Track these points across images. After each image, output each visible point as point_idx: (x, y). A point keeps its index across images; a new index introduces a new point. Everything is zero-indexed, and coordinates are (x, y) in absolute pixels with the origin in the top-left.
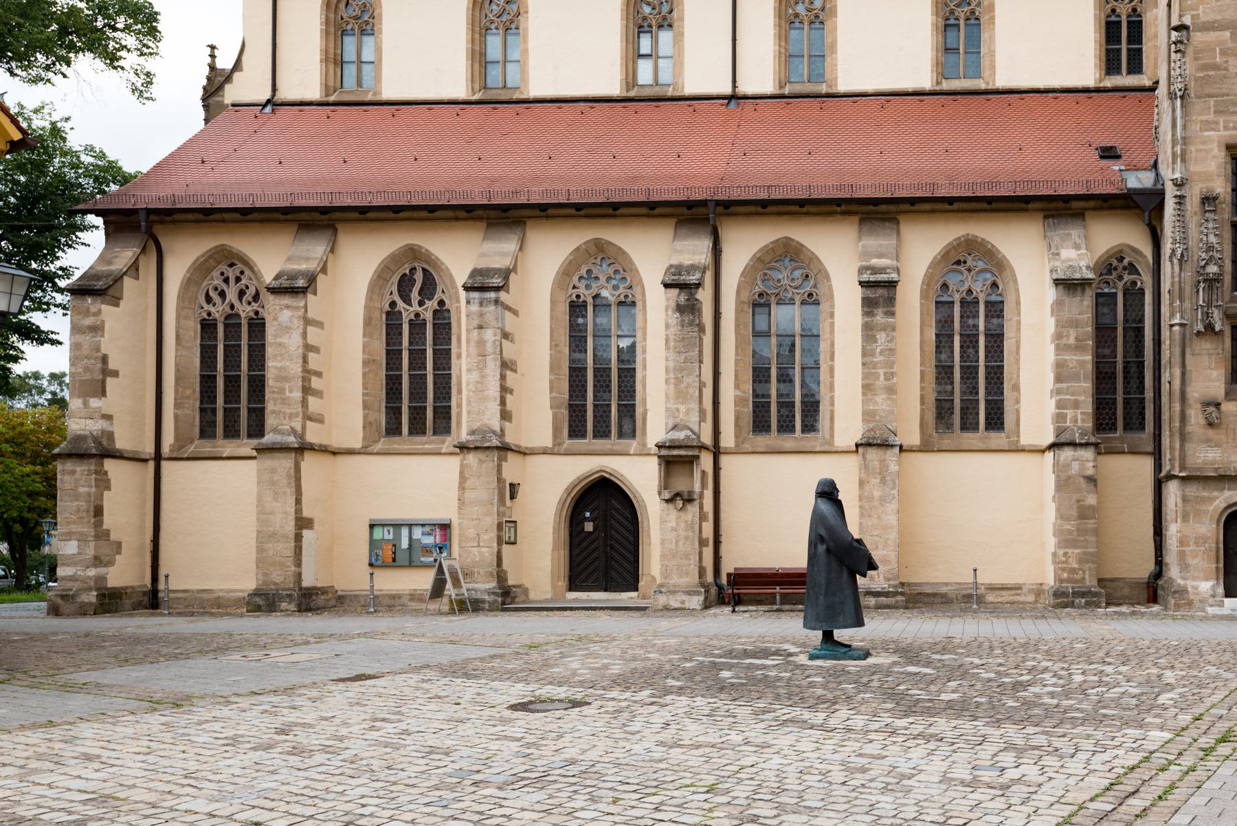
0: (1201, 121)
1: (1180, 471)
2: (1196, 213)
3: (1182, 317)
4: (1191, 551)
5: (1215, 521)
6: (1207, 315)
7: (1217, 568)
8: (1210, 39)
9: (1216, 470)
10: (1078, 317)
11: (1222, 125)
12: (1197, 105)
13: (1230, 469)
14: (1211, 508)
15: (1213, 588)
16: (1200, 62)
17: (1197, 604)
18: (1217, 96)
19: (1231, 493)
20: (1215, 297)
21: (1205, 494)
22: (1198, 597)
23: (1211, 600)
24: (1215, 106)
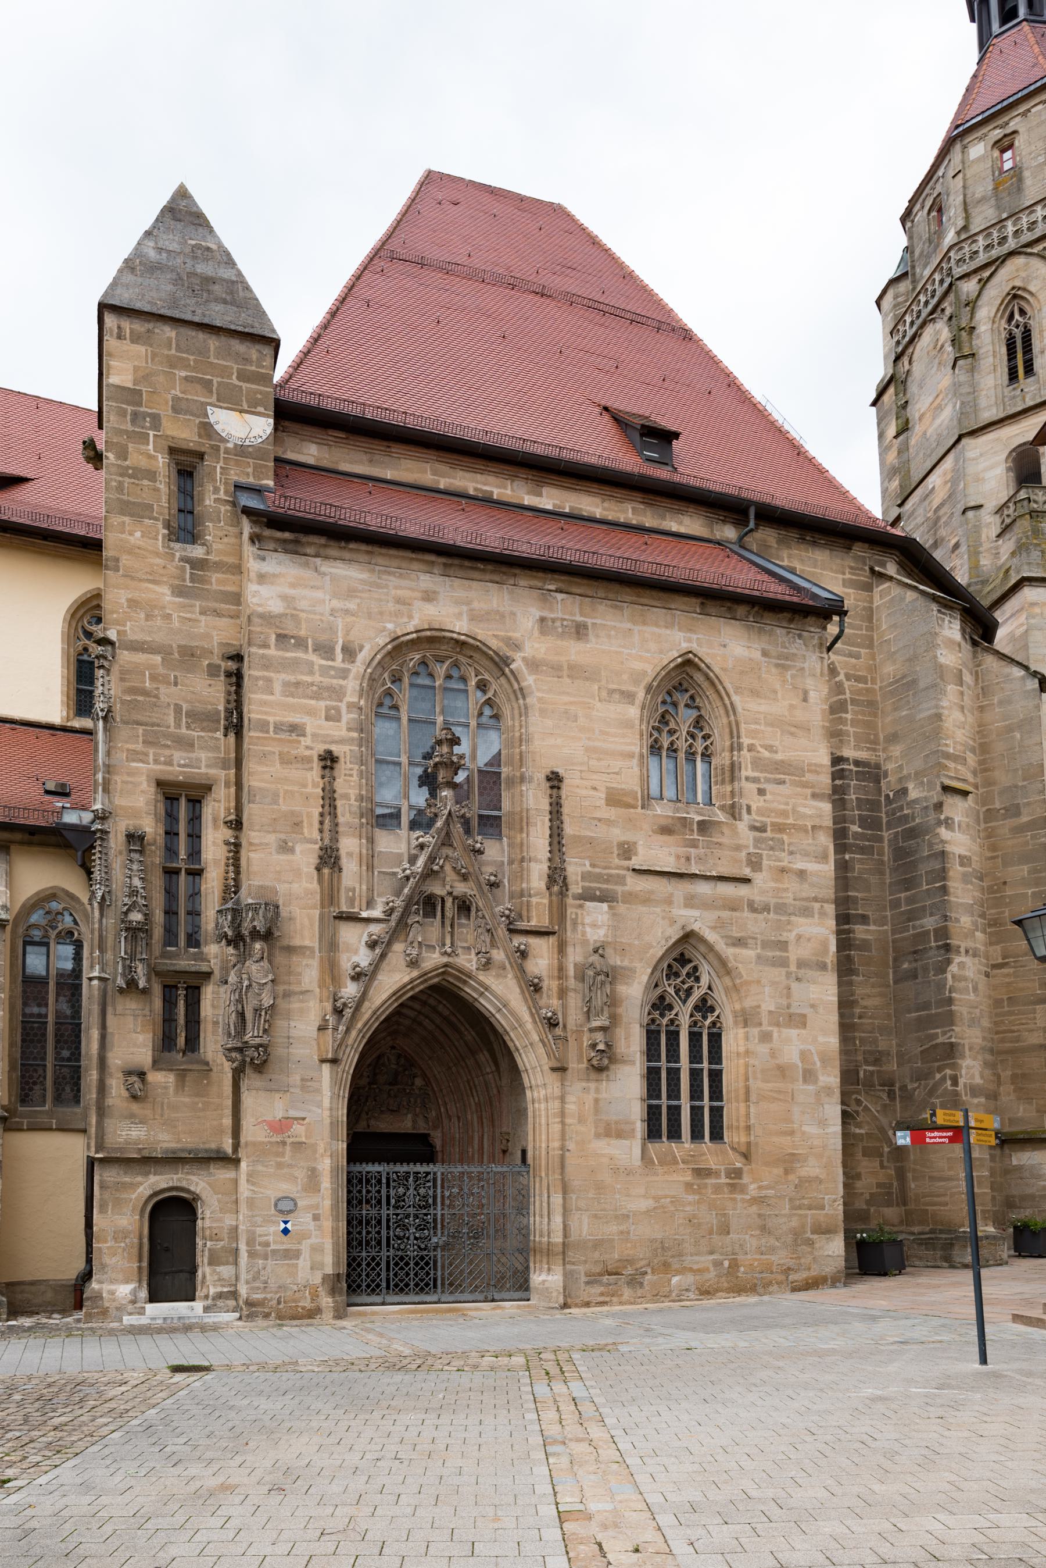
0: (128, 750)
1: (97, 1152)
2: (120, 853)
3: (102, 970)
4: (108, 1248)
5: (138, 1212)
6: (129, 969)
7: (140, 1268)
8: (139, 661)
11: (151, 757)
12: (123, 732)
13: (156, 1150)
14: (133, 1196)
15: (134, 1292)
16: (128, 684)
17: (113, 1312)
18: (146, 725)
20: (139, 949)
21: (127, 1179)
22: (115, 1304)
23: (130, 1307)
24: (143, 735)
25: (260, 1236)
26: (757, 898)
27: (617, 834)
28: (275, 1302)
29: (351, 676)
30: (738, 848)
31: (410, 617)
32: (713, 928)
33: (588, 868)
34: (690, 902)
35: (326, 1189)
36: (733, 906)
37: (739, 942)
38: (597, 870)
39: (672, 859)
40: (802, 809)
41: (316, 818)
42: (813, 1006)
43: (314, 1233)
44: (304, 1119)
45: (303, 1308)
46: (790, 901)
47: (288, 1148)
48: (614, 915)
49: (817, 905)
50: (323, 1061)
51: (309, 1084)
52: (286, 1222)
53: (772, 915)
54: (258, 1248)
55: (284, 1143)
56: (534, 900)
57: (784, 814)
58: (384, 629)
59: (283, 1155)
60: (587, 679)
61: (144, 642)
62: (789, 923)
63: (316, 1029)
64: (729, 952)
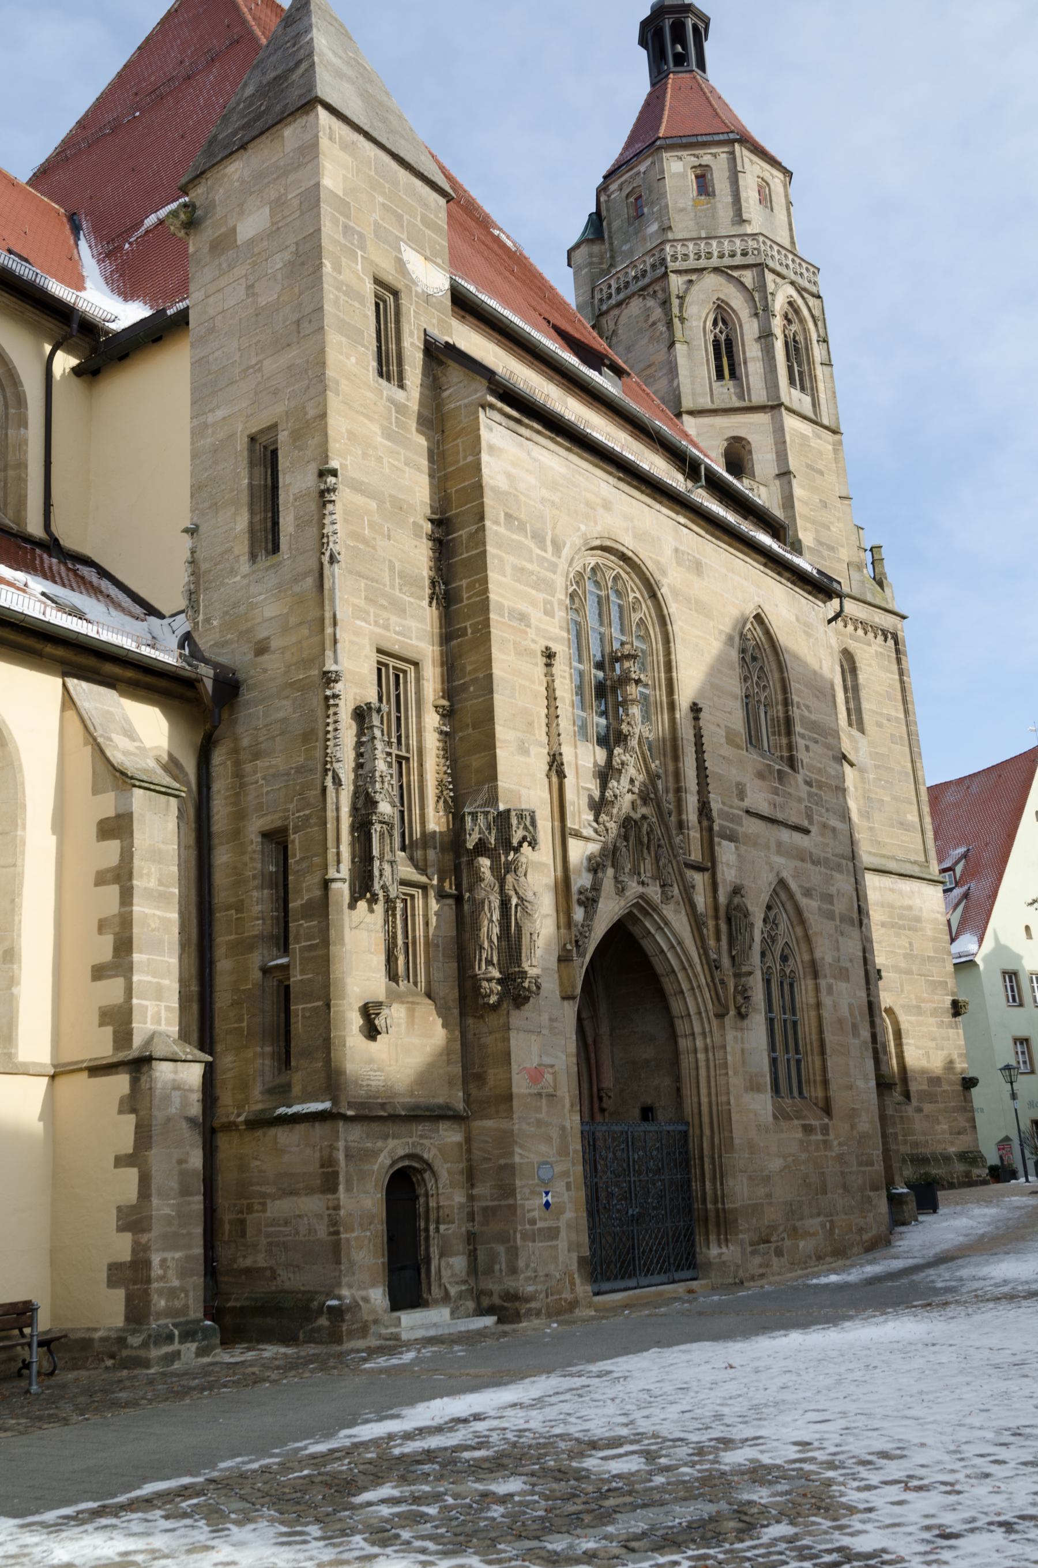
4: (357, 1238)
9: (383, 1106)
10: (163, 847)
19: (396, 1141)
25: (529, 1211)
26: (814, 851)
27: (734, 774)
28: (543, 1295)
29: (559, 571)
30: (800, 800)
31: (596, 523)
32: (793, 877)
33: (721, 806)
35: (575, 1151)
36: (802, 856)
37: (808, 893)
38: (726, 809)
39: (766, 804)
40: (829, 769)
41: (544, 721)
42: (851, 961)
43: (568, 1206)
44: (552, 1066)
45: (566, 1300)
46: (830, 856)
47: (544, 1101)
48: (739, 856)
49: (844, 862)
50: (564, 998)
51: (555, 1024)
52: (547, 1193)
53: (823, 869)
54: (528, 1227)
55: (540, 1095)
56: (692, 833)
57: (820, 771)
58: (579, 529)
59: (538, 1110)
61: (362, 483)
62: (832, 877)
64: (803, 902)
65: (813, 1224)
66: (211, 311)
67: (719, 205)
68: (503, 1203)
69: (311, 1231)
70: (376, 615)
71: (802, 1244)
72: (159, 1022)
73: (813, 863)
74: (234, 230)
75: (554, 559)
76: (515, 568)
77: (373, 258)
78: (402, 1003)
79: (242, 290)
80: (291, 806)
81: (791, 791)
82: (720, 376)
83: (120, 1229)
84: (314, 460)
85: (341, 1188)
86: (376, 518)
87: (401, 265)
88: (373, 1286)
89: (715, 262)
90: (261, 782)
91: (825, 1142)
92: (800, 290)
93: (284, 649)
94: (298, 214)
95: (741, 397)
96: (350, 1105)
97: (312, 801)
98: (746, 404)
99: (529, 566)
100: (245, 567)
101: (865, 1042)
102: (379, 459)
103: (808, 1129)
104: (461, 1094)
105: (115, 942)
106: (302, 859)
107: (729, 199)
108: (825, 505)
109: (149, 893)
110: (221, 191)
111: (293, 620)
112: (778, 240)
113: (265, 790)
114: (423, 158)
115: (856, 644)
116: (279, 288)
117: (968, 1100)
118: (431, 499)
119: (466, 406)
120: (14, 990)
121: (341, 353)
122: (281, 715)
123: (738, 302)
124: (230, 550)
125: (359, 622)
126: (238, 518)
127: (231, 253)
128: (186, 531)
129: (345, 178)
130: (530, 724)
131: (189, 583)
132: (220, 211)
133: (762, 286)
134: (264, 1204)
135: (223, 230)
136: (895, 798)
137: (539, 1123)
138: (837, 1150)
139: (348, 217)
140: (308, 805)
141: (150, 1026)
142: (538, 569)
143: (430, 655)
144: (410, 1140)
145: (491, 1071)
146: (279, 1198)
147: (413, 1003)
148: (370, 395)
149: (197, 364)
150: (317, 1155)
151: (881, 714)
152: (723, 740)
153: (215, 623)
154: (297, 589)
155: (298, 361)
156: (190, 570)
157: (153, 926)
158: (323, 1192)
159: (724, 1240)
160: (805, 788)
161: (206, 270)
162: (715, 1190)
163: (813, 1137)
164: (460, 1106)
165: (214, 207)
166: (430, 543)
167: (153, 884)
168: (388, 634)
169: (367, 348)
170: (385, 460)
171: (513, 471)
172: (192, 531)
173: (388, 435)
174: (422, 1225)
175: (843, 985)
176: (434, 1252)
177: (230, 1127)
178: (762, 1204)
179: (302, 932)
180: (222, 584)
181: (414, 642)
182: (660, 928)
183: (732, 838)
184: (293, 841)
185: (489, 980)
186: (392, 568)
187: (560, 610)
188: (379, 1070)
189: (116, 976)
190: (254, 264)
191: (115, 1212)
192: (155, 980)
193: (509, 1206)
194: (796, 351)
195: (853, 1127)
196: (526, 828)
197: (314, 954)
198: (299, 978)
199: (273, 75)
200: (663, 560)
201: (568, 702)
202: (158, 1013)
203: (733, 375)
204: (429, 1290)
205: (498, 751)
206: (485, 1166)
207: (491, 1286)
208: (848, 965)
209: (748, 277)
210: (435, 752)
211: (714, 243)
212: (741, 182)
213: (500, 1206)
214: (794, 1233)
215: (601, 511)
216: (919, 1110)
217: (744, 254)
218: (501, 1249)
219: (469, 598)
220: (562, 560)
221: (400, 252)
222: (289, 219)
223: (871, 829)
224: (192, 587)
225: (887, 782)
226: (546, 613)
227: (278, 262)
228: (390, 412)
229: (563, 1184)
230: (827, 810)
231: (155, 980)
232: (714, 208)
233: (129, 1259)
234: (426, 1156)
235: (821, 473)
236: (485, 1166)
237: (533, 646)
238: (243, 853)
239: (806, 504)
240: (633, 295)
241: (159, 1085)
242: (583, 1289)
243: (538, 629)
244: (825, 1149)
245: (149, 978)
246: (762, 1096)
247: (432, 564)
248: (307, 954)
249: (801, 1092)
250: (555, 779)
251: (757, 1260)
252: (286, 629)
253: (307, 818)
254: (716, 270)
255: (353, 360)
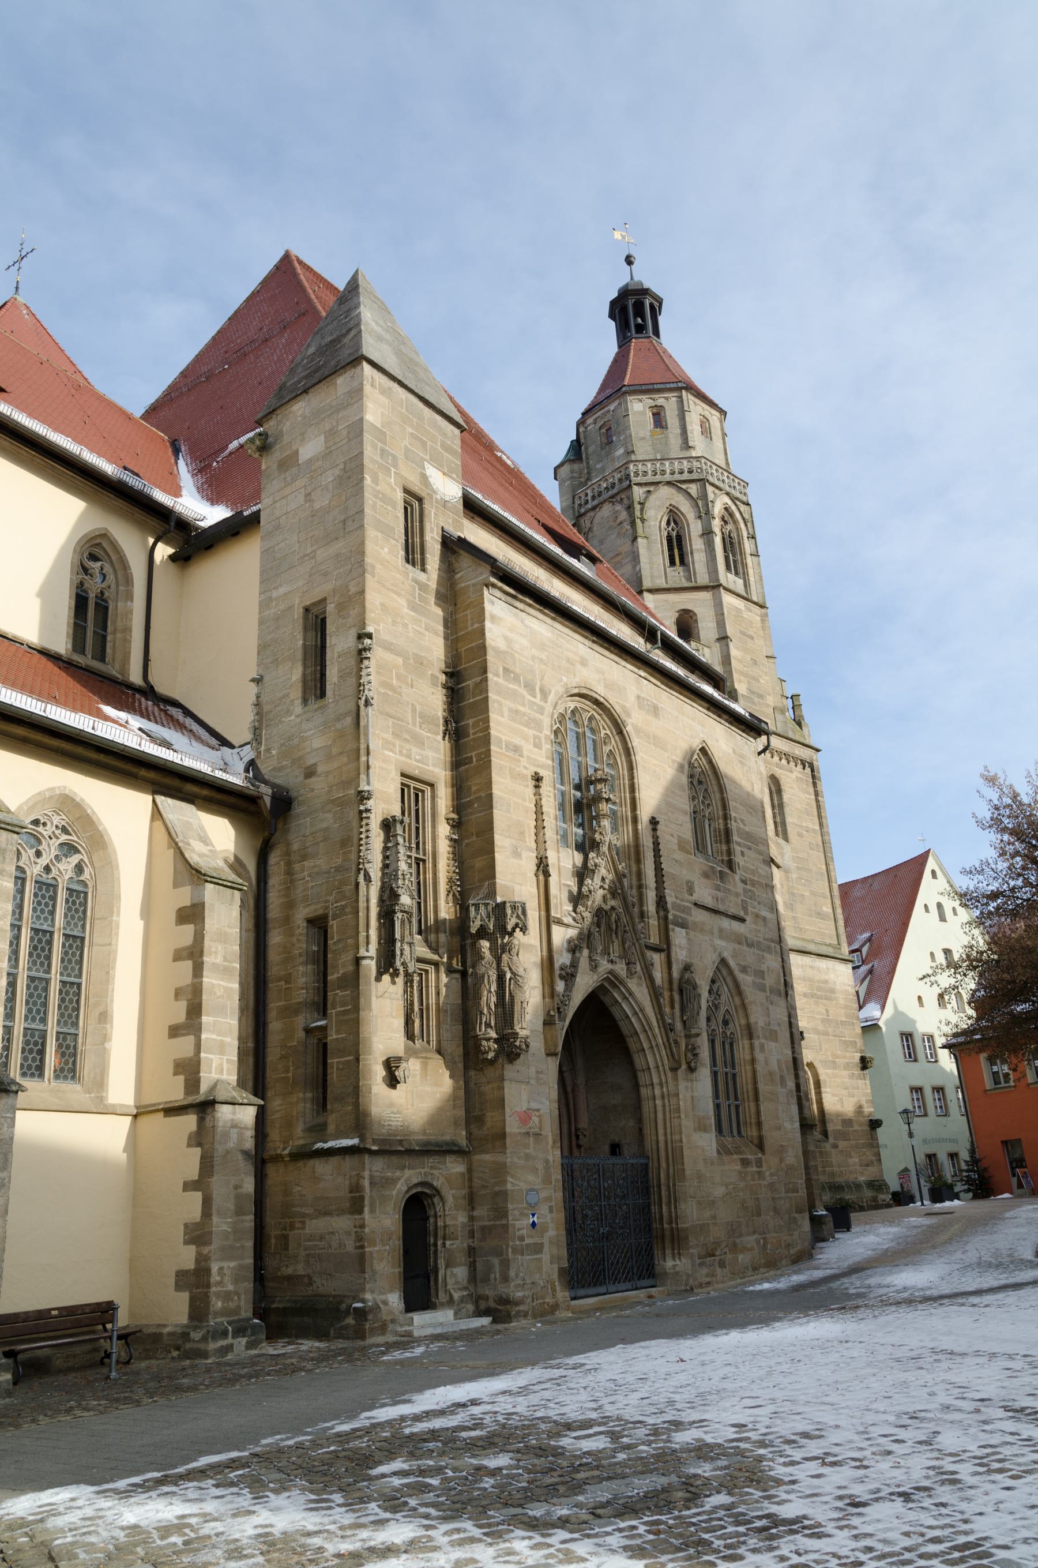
4: (378, 1251)
9: (401, 1142)
10: (228, 930)
19: (411, 1172)
25: (519, 1230)
26: (748, 936)
28: (529, 1300)
29: (546, 713)
30: (737, 895)
31: (575, 675)
32: (732, 957)
33: (674, 899)
34: (722, 934)
35: (557, 1180)
36: (739, 939)
37: (744, 970)
38: (678, 902)
39: (710, 899)
40: (760, 871)
41: (533, 830)
42: (779, 1024)
43: (551, 1225)
44: (538, 1110)
45: (548, 1304)
46: (761, 940)
47: (531, 1139)
48: (689, 939)
49: (773, 945)
50: (548, 1055)
51: (541, 1076)
52: (533, 1215)
54: (518, 1243)
55: (528, 1134)
56: (651, 921)
57: (753, 872)
58: (561, 680)
59: (527, 1146)
60: (662, 749)
63: (541, 1023)
64: (741, 977)
65: (750, 1240)
66: (278, 513)
67: (671, 436)
68: (497, 1223)
69: (341, 1245)
70: (401, 747)
71: (741, 1257)
72: (221, 1072)
73: (748, 945)
74: (297, 452)
75: (542, 704)
76: (510, 710)
77: (403, 473)
78: (418, 1058)
79: (301, 498)
80: (331, 898)
81: (730, 887)
82: (672, 563)
83: (186, 1243)
84: (354, 626)
85: (366, 1209)
86: (402, 671)
87: (424, 478)
88: (391, 1291)
89: (668, 477)
90: (307, 878)
91: (759, 1173)
92: (733, 499)
93: (328, 773)
94: (346, 441)
95: (689, 579)
96: (374, 1142)
97: (348, 894)
98: (693, 584)
99: (522, 709)
100: (298, 708)
101: (791, 1091)
102: (405, 626)
103: (745, 1162)
104: (464, 1133)
105: (188, 1007)
106: (339, 941)
107: (679, 431)
108: (755, 662)
109: (215, 967)
110: (288, 423)
111: (335, 751)
112: (716, 461)
113: (310, 885)
114: (442, 399)
115: (781, 771)
116: (329, 496)
117: (874, 1138)
118: (446, 656)
119: (473, 585)
120: (107, 1045)
121: (377, 545)
122: (324, 825)
123: (685, 507)
124: (287, 695)
125: (387, 752)
126: (294, 671)
127: (294, 470)
128: (253, 680)
129: (383, 415)
130: (522, 833)
131: (254, 721)
132: (286, 439)
133: (704, 496)
134: (303, 1223)
135: (288, 452)
136: (813, 893)
137: (528, 1157)
138: (768, 1179)
139: (385, 443)
140: (344, 897)
141: (214, 1076)
142: (529, 711)
143: (443, 778)
144: (423, 1171)
145: (489, 1114)
146: (316, 1218)
147: (426, 1058)
148: (398, 576)
149: (265, 553)
150: (347, 1182)
151: (801, 826)
152: (676, 847)
153: (274, 752)
154: (339, 726)
155: (344, 551)
156: (255, 711)
157: (218, 994)
158: (352, 1213)
159: (677, 1254)
160: (741, 885)
161: (274, 482)
162: (670, 1212)
163: (749, 1169)
164: (464, 1143)
165: (282, 436)
166: (444, 691)
167: (219, 960)
168: (409, 761)
169: (397, 541)
170: (410, 626)
171: (510, 635)
172: (257, 681)
173: (413, 607)
174: (432, 1241)
175: (773, 1044)
176: (442, 1264)
177: (277, 1159)
178: (708, 1224)
179: (338, 1000)
180: (280, 722)
181: (431, 768)
182: (625, 998)
183: (683, 925)
184: (332, 926)
185: (488, 1040)
186: (414, 710)
187: (546, 743)
188: (398, 1112)
189: (188, 1034)
190: (312, 478)
191: (182, 1228)
192: (219, 1038)
193: (503, 1225)
194: (731, 545)
195: (781, 1160)
196: (518, 917)
197: (346, 1017)
198: (335, 1037)
199: (330, 339)
200: (627, 705)
201: (552, 816)
202: (221, 1065)
203: (683, 562)
204: (437, 1295)
205: (496, 855)
206: (483, 1192)
207: (487, 1292)
208: (777, 1028)
209: (693, 489)
210: (446, 855)
211: (667, 463)
212: (687, 419)
213: (495, 1225)
214: (734, 1248)
215: (579, 666)
216: (835, 1146)
217: (690, 472)
218: (496, 1261)
219: (474, 734)
220: (549, 704)
221: (424, 469)
222: (339, 445)
223: (794, 918)
224: (257, 724)
225: (806, 880)
226: (535, 745)
227: (329, 477)
228: (414, 590)
229: (547, 1207)
230: (759, 903)
231: (219, 1038)
232: (667, 437)
233: (193, 1267)
234: (435, 1184)
235: (752, 638)
236: (483, 1192)
237: (525, 772)
238: (292, 935)
239: (740, 661)
240: (605, 501)
241: (220, 1124)
242: (562, 1295)
243: (528, 758)
244: (759, 1179)
245: (214, 1037)
246: (706, 1136)
247: (445, 707)
248: (341, 1018)
249: (739, 1132)
250: (541, 878)
251: (704, 1271)
252: (329, 758)
253: (343, 907)
254: (669, 483)
255: (386, 550)
